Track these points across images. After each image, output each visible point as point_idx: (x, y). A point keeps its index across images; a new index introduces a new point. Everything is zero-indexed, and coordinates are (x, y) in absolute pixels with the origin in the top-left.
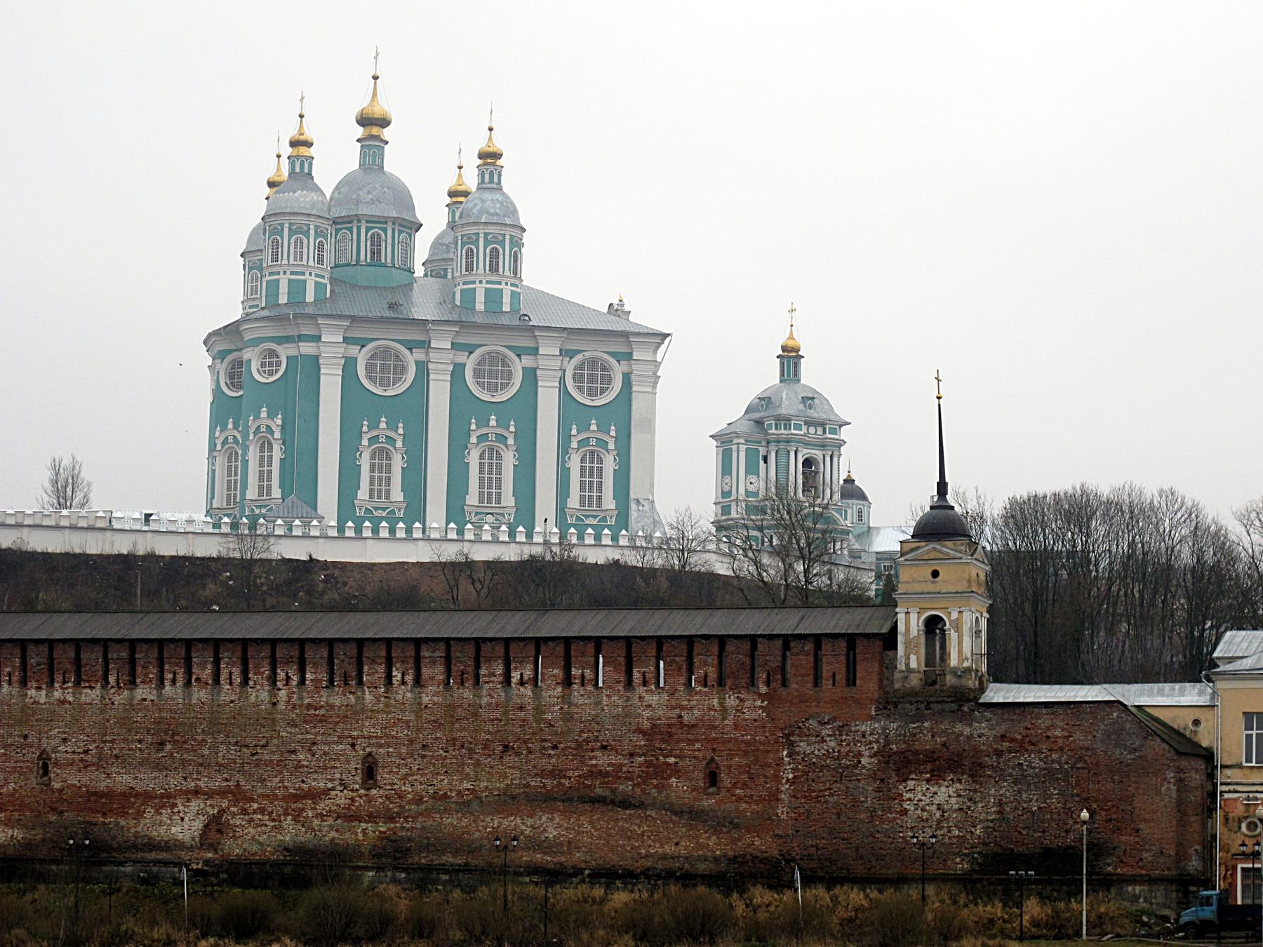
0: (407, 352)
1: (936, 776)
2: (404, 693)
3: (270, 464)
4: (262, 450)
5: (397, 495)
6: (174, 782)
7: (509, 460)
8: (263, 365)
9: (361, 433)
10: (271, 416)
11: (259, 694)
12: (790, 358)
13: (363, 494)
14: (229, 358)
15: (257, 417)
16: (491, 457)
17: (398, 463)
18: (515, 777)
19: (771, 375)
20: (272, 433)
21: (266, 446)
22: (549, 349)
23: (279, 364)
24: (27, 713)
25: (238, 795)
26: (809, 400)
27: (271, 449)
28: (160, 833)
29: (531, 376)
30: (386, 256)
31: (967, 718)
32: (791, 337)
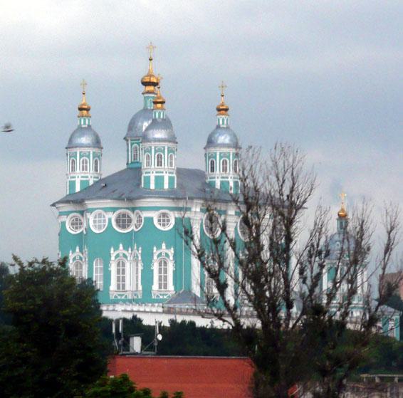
20: (169, 257)
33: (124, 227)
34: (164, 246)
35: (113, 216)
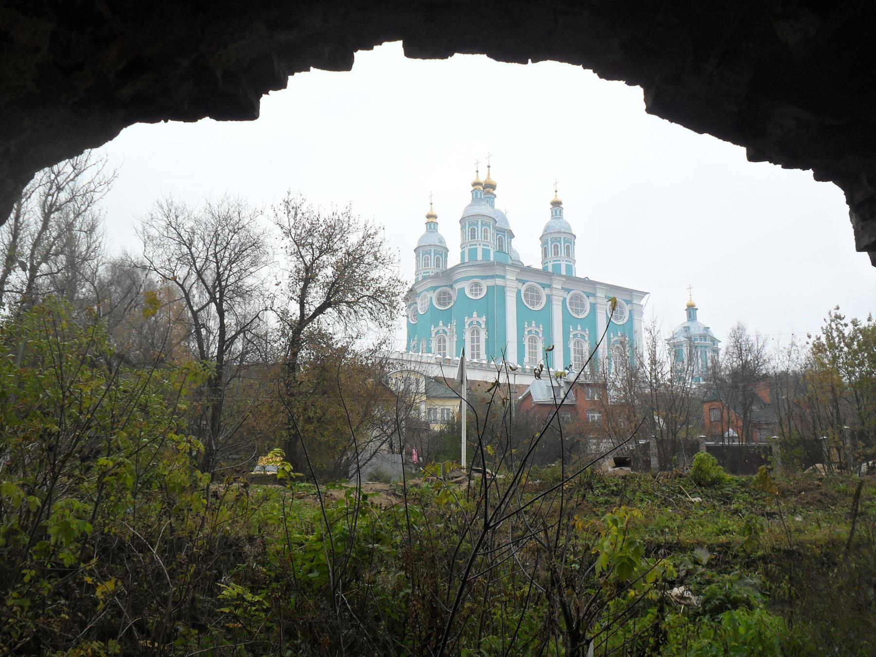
0: (542, 289)
3: (478, 341)
4: (473, 334)
8: (471, 290)
9: (524, 328)
10: (479, 316)
12: (691, 310)
14: (438, 290)
15: (471, 316)
20: (480, 325)
21: (475, 332)
23: (481, 290)
27: (478, 333)
32: (691, 300)
33: (445, 305)
34: (475, 314)
35: (434, 295)
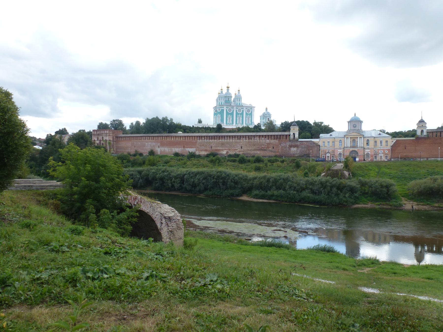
1: (294, 147)
2: (245, 140)
5: (231, 122)
6: (223, 148)
7: (241, 119)
11: (231, 140)
12: (267, 109)
13: (228, 122)
16: (239, 118)
17: (231, 119)
18: (255, 148)
19: (265, 111)
21: (219, 118)
22: (245, 108)
24: (210, 142)
25: (229, 150)
26: (268, 113)
28: (222, 153)
29: (243, 111)
30: (229, 100)
31: (297, 142)
